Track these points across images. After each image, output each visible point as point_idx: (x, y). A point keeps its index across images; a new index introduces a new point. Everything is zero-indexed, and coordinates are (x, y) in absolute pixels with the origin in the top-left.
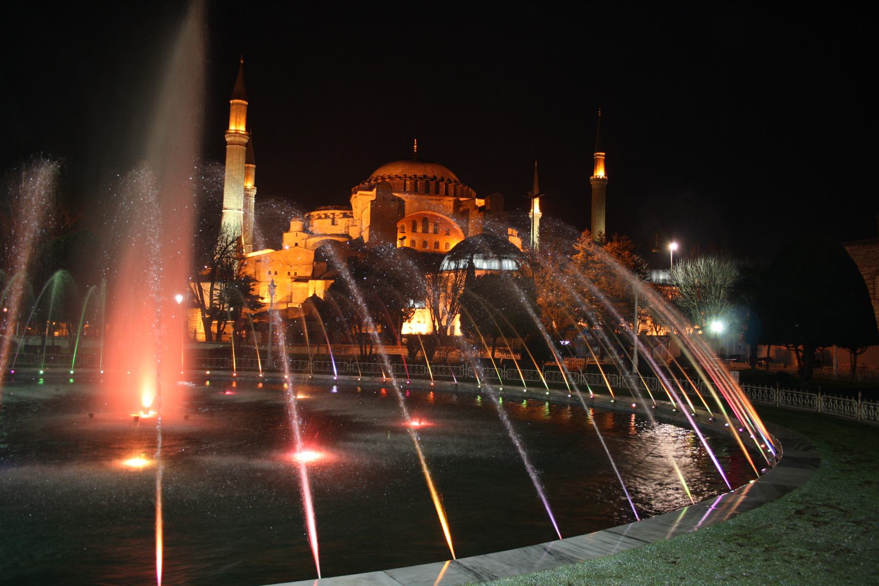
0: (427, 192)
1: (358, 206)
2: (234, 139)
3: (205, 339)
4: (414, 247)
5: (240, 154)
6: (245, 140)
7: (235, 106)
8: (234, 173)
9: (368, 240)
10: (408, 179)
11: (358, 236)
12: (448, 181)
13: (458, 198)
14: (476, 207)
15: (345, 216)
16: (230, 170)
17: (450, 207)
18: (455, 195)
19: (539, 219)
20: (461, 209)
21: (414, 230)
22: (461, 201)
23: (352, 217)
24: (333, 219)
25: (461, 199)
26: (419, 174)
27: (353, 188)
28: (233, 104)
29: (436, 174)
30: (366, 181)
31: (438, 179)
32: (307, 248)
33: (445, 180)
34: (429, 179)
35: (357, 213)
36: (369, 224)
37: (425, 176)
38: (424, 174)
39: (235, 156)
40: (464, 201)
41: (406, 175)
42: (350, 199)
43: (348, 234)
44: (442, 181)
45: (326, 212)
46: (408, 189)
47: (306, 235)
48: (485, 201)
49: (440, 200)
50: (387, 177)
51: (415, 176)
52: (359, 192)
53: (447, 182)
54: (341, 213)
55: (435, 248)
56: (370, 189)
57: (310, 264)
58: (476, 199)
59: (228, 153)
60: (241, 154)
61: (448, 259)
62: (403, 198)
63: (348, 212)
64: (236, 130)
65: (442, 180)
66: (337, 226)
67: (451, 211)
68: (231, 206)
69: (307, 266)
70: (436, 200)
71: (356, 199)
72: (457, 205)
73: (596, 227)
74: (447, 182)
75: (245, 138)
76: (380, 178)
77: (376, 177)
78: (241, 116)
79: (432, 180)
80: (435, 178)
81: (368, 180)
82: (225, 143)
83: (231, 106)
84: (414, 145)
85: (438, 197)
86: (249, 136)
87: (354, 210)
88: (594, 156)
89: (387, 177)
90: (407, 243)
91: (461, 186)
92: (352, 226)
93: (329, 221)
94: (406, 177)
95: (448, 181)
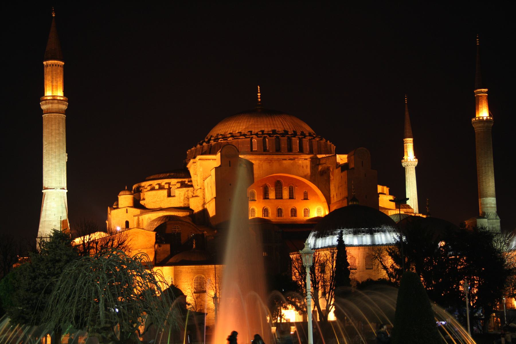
0: (278, 150)
1: (199, 174)
2: (52, 106)
3: (68, 343)
4: (267, 216)
5: (59, 123)
6: (64, 107)
7: (49, 67)
8: (53, 146)
9: (214, 214)
10: (254, 136)
11: (201, 209)
12: (301, 135)
13: (316, 155)
14: (338, 165)
15: (183, 185)
16: (49, 143)
17: (307, 166)
18: (311, 152)
19: (414, 167)
20: (320, 168)
21: (266, 197)
22: (319, 159)
23: (192, 186)
24: (169, 189)
25: (319, 156)
26: (267, 129)
27: (189, 150)
28: (47, 66)
29: (287, 128)
30: (204, 141)
31: (289, 133)
32: (141, 225)
33: (298, 134)
34: (279, 134)
35: (197, 181)
36: (214, 195)
37: (274, 132)
38: (273, 129)
39: (53, 126)
40: (322, 158)
41: (251, 132)
42: (186, 164)
43: (189, 207)
44: (295, 137)
45: (159, 181)
46: (255, 148)
47: (137, 211)
48: (348, 157)
49: (294, 159)
50: (230, 135)
51: (263, 131)
52: (199, 157)
53: (300, 137)
54: (178, 182)
55: (292, 216)
56: (211, 151)
57: (151, 248)
58: (337, 155)
59: (45, 123)
60: (61, 124)
61: (314, 235)
62: (249, 160)
63: (186, 180)
64: (52, 96)
65: (295, 134)
66: (174, 198)
67: (308, 171)
68: (53, 185)
69: (148, 250)
70: (289, 159)
71: (195, 164)
72: (315, 162)
73: (484, 178)
74: (300, 137)
75: (64, 104)
76: (220, 137)
77: (215, 135)
78: (58, 80)
79: (283, 135)
80: (286, 132)
81: (206, 140)
82: (41, 112)
83: (45, 68)
84: (258, 93)
85: (290, 156)
86: (68, 101)
87: (193, 178)
88: (474, 94)
89: (230, 135)
90: (258, 214)
91: (317, 139)
92: (193, 197)
93: (165, 192)
94: (251, 134)
95: (301, 135)
